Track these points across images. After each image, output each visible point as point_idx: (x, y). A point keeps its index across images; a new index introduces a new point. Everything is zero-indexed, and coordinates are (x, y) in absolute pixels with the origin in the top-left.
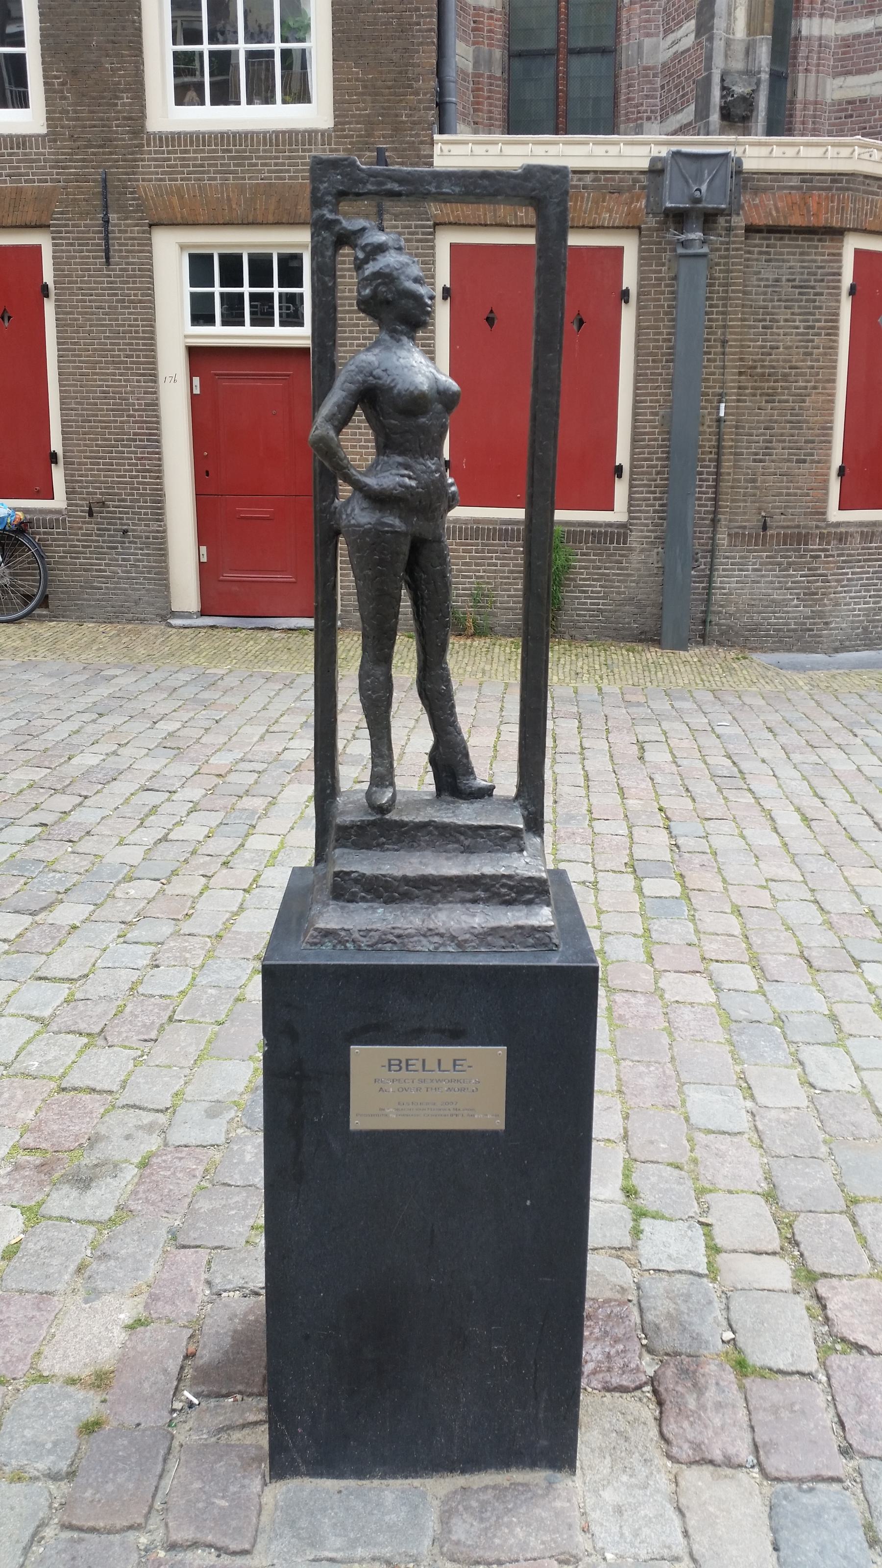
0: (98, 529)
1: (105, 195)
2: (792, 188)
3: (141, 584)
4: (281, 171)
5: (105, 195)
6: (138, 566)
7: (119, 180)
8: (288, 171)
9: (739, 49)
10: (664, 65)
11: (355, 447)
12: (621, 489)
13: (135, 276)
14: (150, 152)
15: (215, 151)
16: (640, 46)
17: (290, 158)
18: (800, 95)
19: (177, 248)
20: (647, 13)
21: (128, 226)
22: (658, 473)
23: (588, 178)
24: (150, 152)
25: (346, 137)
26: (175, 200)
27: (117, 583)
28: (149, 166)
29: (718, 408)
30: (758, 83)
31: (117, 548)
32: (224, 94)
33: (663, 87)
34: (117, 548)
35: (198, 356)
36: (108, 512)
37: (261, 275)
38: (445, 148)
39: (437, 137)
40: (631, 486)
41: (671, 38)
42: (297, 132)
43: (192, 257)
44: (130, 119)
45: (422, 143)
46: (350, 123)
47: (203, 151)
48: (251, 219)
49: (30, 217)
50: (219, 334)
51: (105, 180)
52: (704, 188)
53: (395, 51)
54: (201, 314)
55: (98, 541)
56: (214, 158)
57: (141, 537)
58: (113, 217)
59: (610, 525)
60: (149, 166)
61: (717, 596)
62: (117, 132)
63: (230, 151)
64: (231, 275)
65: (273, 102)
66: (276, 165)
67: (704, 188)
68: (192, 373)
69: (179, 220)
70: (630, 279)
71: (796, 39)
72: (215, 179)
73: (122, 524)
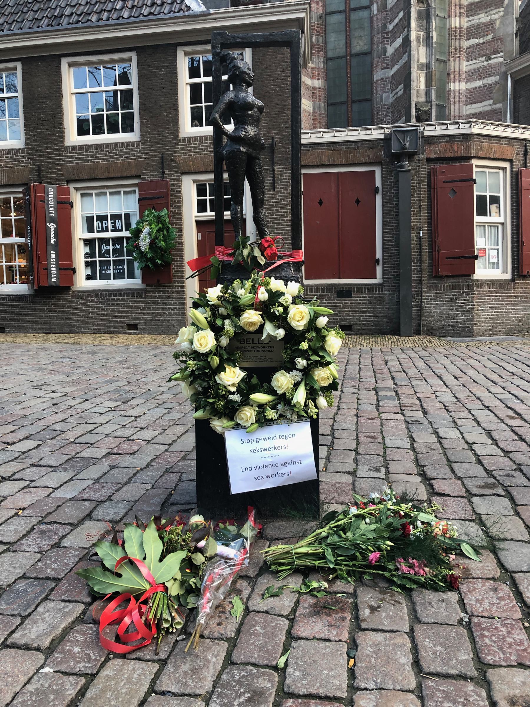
1: (162, 163)
2: (446, 142)
5: (162, 163)
9: (423, 93)
10: (392, 103)
12: (379, 270)
15: (207, 143)
16: (382, 97)
18: (452, 113)
20: (384, 84)
22: (395, 261)
23: (359, 144)
26: (191, 163)
29: (420, 233)
30: (431, 106)
33: (392, 112)
35: (200, 224)
40: (383, 267)
41: (394, 92)
49: (134, 172)
51: (162, 157)
52: (408, 144)
58: (166, 171)
59: (375, 284)
61: (425, 314)
67: (408, 144)
68: (198, 231)
70: (378, 183)
71: (448, 91)
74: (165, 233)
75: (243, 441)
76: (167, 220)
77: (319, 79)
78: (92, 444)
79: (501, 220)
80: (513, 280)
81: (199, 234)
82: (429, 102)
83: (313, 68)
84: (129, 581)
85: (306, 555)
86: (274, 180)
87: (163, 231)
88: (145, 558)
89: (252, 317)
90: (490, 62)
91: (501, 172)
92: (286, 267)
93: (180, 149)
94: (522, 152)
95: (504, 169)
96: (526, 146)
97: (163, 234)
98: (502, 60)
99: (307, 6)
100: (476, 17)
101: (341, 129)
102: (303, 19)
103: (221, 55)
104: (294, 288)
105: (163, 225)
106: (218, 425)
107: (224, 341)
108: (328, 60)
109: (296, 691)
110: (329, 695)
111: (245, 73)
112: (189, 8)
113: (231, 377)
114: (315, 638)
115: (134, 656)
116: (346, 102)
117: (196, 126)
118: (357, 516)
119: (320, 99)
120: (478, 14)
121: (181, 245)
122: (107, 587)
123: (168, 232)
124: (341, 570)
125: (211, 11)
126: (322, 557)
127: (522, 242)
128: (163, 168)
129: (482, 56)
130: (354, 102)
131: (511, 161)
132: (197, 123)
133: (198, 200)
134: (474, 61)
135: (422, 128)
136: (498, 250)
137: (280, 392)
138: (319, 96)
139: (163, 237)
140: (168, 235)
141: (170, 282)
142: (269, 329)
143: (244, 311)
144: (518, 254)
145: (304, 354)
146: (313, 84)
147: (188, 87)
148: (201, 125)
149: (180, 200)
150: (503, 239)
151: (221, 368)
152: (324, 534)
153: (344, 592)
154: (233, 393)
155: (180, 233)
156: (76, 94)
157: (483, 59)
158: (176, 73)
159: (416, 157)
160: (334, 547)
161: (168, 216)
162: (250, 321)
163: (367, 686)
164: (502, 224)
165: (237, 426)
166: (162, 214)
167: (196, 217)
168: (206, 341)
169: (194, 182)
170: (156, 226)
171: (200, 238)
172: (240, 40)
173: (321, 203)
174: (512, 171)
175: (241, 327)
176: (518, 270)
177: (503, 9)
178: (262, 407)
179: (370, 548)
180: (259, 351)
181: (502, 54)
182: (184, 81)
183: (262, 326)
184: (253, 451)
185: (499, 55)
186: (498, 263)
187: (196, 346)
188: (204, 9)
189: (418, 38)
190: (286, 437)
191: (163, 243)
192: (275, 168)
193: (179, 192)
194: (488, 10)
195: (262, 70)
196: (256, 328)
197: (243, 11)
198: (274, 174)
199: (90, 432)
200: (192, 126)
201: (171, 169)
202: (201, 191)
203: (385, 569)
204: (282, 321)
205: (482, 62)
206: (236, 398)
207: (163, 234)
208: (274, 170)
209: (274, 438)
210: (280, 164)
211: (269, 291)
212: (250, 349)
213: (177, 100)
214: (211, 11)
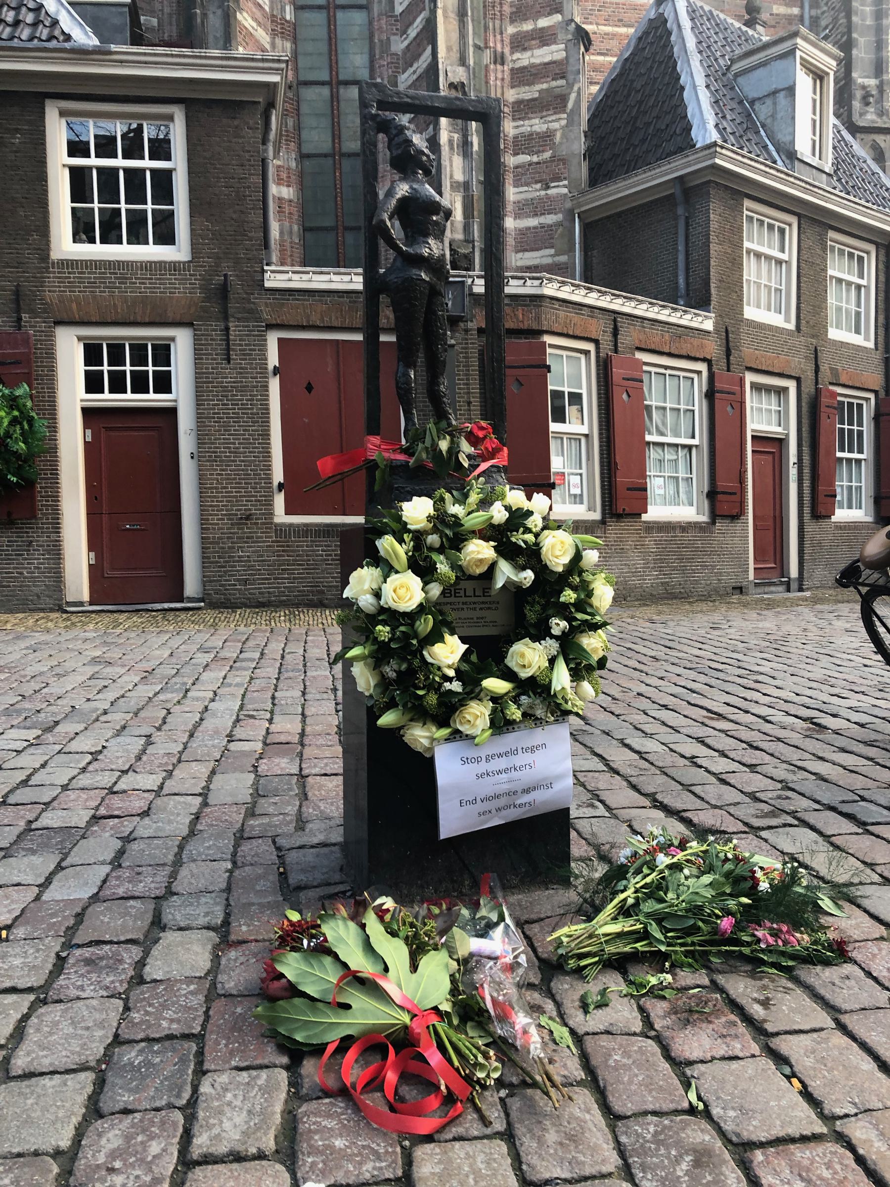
5: (17, 301)
9: (460, 227)
14: (54, 273)
24: (54, 273)
26: (74, 306)
32: (110, 235)
35: (90, 414)
37: (139, 357)
38: (273, 275)
39: (266, 268)
42: (165, 262)
50: (107, 398)
51: (18, 291)
53: (235, 212)
54: (93, 384)
58: (25, 316)
68: (86, 427)
75: (465, 761)
77: (289, 186)
78: (47, 804)
79: (584, 430)
80: (603, 522)
82: (469, 241)
83: (279, 167)
84: (365, 1014)
85: (620, 935)
86: (228, 345)
87: (21, 424)
88: (386, 969)
89: (480, 551)
90: (549, 192)
91: (583, 357)
93: (52, 278)
94: (610, 330)
95: (586, 353)
96: (615, 320)
97: (22, 428)
98: (565, 191)
99: (283, 65)
100: (527, 122)
101: (342, 270)
102: (275, 84)
103: (378, 119)
105: (21, 412)
106: (420, 736)
107: (435, 590)
108: (303, 157)
109: (754, 1138)
110: (805, 1133)
111: (423, 153)
112: (68, 38)
113: (449, 652)
114: (713, 1058)
115: (449, 1136)
116: (335, 229)
117: (81, 241)
118: (671, 867)
119: (290, 218)
120: (529, 119)
121: (53, 450)
122: (324, 1031)
123: (31, 425)
124: (675, 952)
125: (113, 47)
126: (644, 935)
127: (616, 464)
128: (18, 310)
129: (536, 182)
130: (346, 228)
131: (596, 342)
132: (84, 237)
134: (526, 188)
135: (470, 281)
136: (581, 475)
137: (524, 674)
138: (290, 213)
139: (22, 434)
141: (34, 517)
142: (505, 572)
143: (466, 540)
144: (610, 482)
145: (564, 611)
146: (280, 192)
147: (67, 172)
148: (92, 241)
149: (52, 369)
150: (588, 459)
151: (435, 637)
152: (631, 901)
153: (698, 986)
154: (450, 680)
155: (53, 428)
157: (538, 186)
158: (44, 144)
159: (462, 324)
160: (660, 919)
161: (31, 396)
162: (480, 556)
163: (846, 1111)
164: (586, 436)
165: (457, 735)
166: (19, 392)
167: (82, 400)
168: (406, 591)
169: (80, 339)
171: (89, 439)
172: (409, 100)
173: (309, 388)
174: (598, 357)
176: (610, 506)
177: (565, 116)
178: (496, 699)
179: (717, 911)
180: (475, 609)
181: (566, 182)
183: (493, 566)
184: (480, 776)
185: (561, 183)
186: (581, 495)
187: (389, 599)
188: (96, 42)
189: (451, 142)
190: (533, 749)
191: (22, 445)
192: (231, 324)
193: (50, 355)
194: (544, 113)
195: (205, 158)
196: (484, 568)
197: (172, 56)
198: (228, 335)
199: (25, 783)
200: (74, 242)
201: (33, 313)
202: (92, 354)
203: (738, 942)
204: (530, 557)
205: (537, 190)
206: (456, 686)
207: (22, 428)
208: (227, 329)
209: (515, 752)
210: (239, 320)
211: (508, 508)
212: (461, 606)
213: (45, 192)
214: (113, 47)
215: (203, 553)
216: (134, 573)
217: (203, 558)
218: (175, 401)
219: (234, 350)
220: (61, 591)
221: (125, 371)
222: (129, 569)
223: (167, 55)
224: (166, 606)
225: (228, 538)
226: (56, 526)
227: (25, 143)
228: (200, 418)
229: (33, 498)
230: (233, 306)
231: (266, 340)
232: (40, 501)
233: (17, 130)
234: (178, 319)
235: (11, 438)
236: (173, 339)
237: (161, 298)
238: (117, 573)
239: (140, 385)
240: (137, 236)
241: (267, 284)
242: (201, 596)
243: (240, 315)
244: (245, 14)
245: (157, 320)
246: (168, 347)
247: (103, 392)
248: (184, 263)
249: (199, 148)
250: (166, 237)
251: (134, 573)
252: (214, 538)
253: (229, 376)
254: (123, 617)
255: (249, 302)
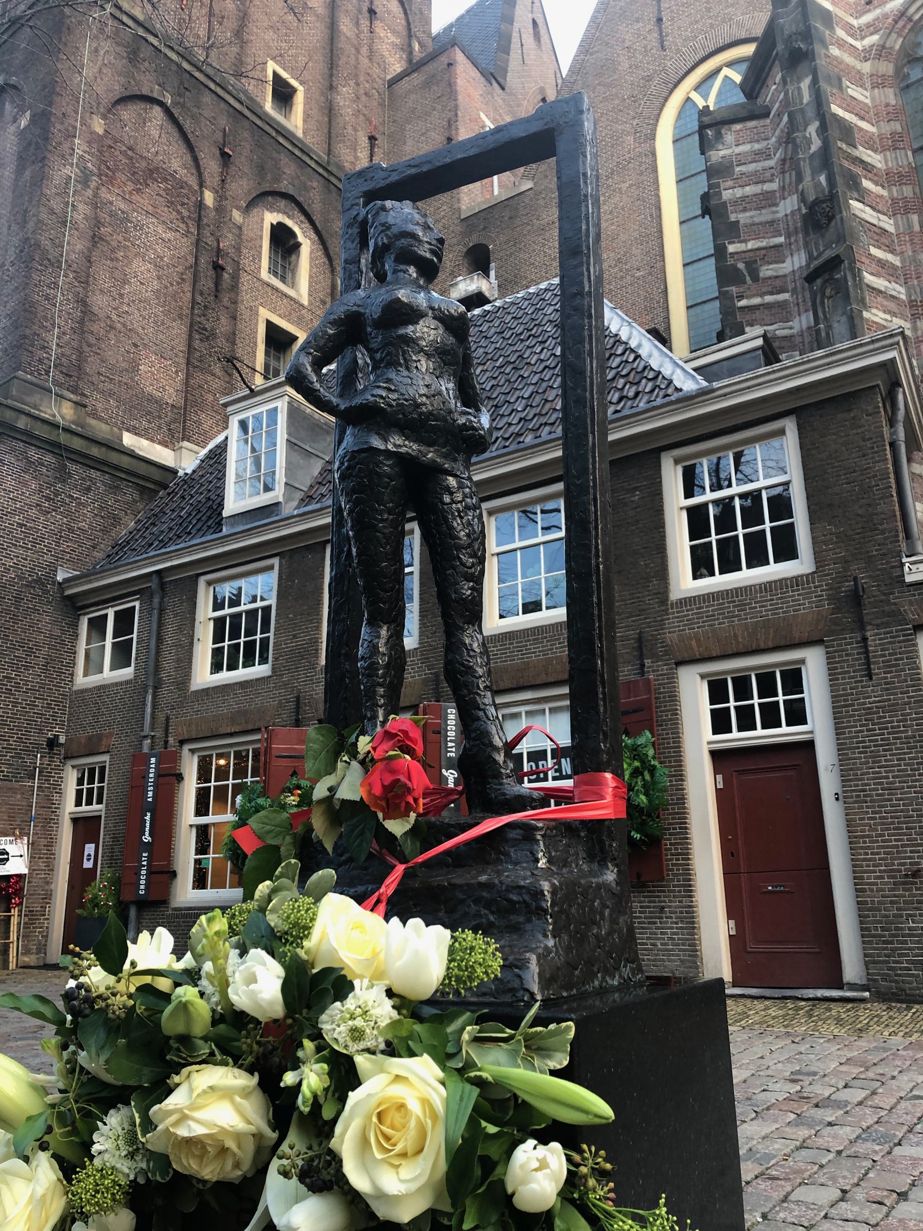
0: (641, 907)
1: (640, 648)
3: (678, 955)
4: (777, 609)
5: (640, 648)
6: (674, 939)
7: (652, 635)
8: (782, 608)
11: (863, 819)
13: (666, 702)
14: (673, 613)
15: (723, 604)
17: (782, 598)
19: (698, 678)
21: (659, 666)
24: (673, 613)
25: (827, 575)
26: (694, 643)
27: (657, 955)
28: (673, 622)
31: (655, 923)
32: (730, 565)
34: (655, 923)
35: (717, 756)
36: (649, 892)
37: (767, 688)
38: (913, 567)
42: (786, 579)
43: (710, 684)
44: (659, 593)
45: (893, 567)
46: (828, 565)
47: (713, 605)
48: (754, 647)
50: (736, 737)
53: (860, 507)
54: (720, 723)
55: (640, 917)
56: (722, 609)
57: (676, 913)
58: (648, 662)
60: (673, 622)
62: (649, 604)
63: (734, 602)
64: (743, 691)
65: (768, 563)
66: (771, 605)
69: (698, 657)
72: (724, 623)
73: (660, 902)
74: (647, 777)
76: (651, 752)
81: (719, 778)
86: (867, 658)
87: (642, 774)
92: (515, 843)
93: (672, 621)
97: (644, 780)
102: (893, 361)
104: (421, 952)
105: (643, 762)
117: (702, 576)
121: (681, 800)
123: (652, 775)
125: (715, 385)
128: (641, 657)
132: (704, 571)
133: (712, 710)
139: (644, 786)
140: (654, 782)
141: (663, 879)
147: (684, 515)
148: (712, 574)
149: (675, 713)
155: (679, 775)
156: (498, 554)
161: (653, 744)
166: (641, 741)
167: (709, 743)
169: (703, 677)
170: (630, 765)
171: (720, 786)
175: (162, 1160)
182: (675, 503)
191: (643, 797)
192: (868, 634)
193: (673, 698)
197: (774, 372)
198: (866, 647)
201: (655, 657)
202: (717, 691)
207: (644, 780)
208: (865, 639)
210: (878, 626)
214: (715, 385)
215: (861, 922)
216: (779, 948)
217: (862, 929)
218: (811, 732)
219: (875, 663)
220: (697, 967)
221: (753, 705)
222: (773, 942)
223: (769, 373)
224: (820, 993)
225: (892, 902)
226: (688, 889)
227: (642, 498)
228: (842, 749)
229: (659, 858)
230: (868, 612)
231: (915, 645)
232: (670, 860)
233: (636, 489)
234: (805, 637)
235: (632, 790)
236: (803, 661)
237: (784, 618)
238: (762, 947)
239: (771, 720)
240: (757, 558)
241: (909, 579)
242: (864, 982)
243: (879, 621)
244: (874, 311)
245: (783, 643)
246: (799, 671)
247: (729, 731)
248: (807, 575)
249: (813, 452)
250: (786, 551)
251: (779, 948)
252: (873, 902)
253: (873, 695)
254: (759, 1005)
255: (888, 602)
